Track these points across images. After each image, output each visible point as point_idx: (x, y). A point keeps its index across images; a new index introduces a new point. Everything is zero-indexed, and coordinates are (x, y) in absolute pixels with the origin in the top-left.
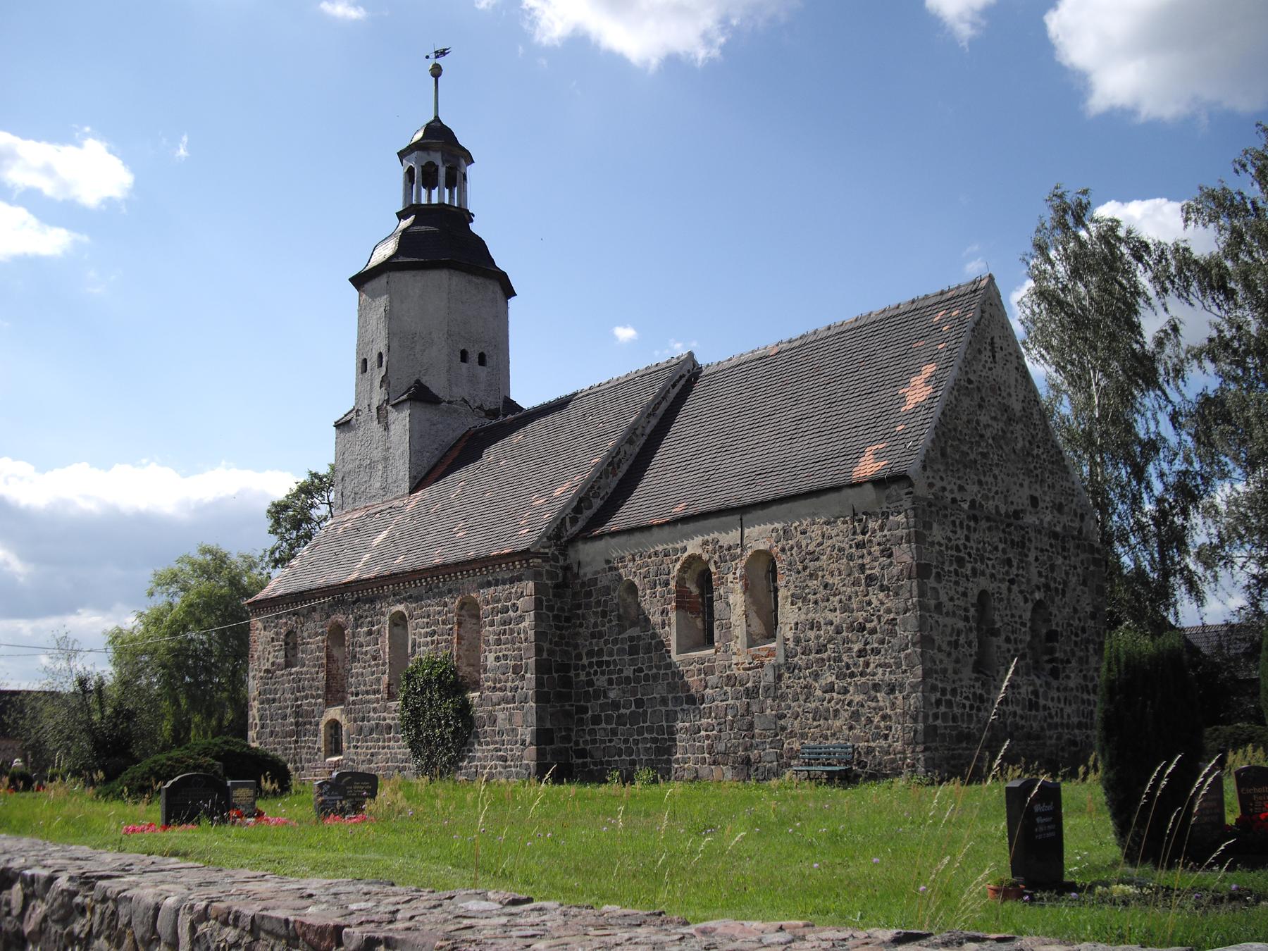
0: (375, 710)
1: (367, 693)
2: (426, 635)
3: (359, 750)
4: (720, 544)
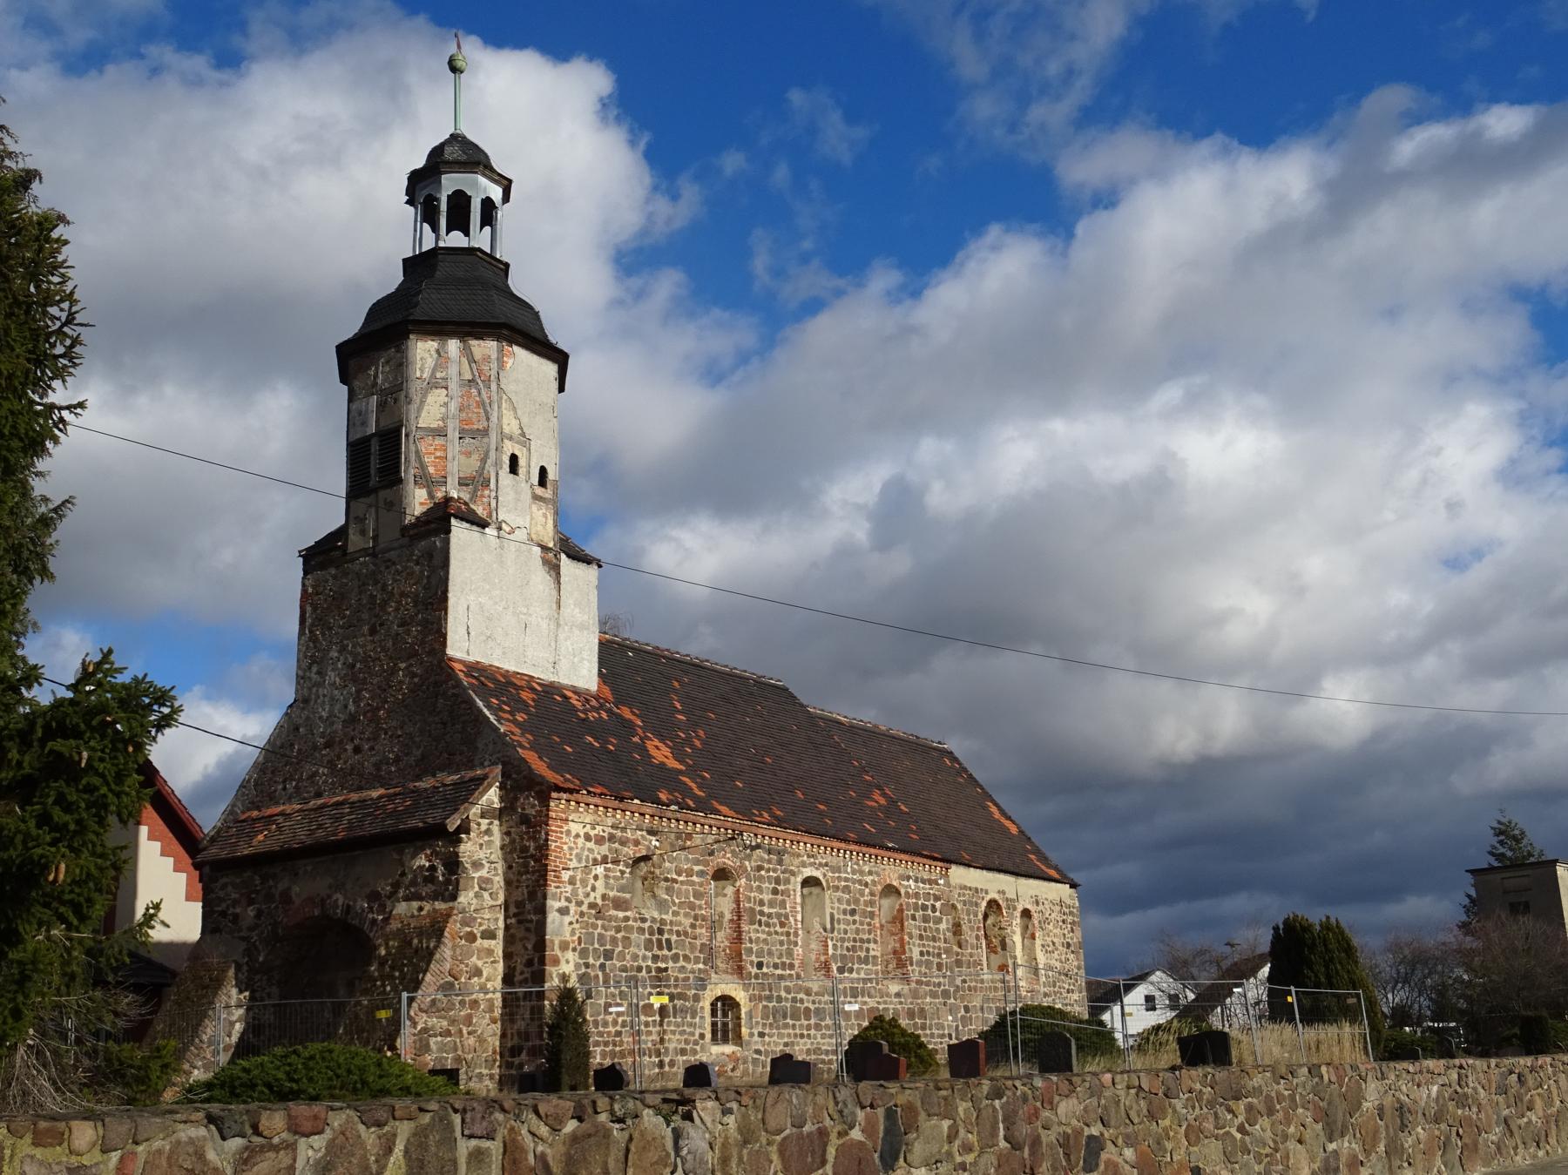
0: (788, 990)
1: (776, 966)
2: (845, 912)
3: (767, 1039)
4: (1007, 895)
